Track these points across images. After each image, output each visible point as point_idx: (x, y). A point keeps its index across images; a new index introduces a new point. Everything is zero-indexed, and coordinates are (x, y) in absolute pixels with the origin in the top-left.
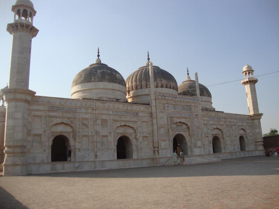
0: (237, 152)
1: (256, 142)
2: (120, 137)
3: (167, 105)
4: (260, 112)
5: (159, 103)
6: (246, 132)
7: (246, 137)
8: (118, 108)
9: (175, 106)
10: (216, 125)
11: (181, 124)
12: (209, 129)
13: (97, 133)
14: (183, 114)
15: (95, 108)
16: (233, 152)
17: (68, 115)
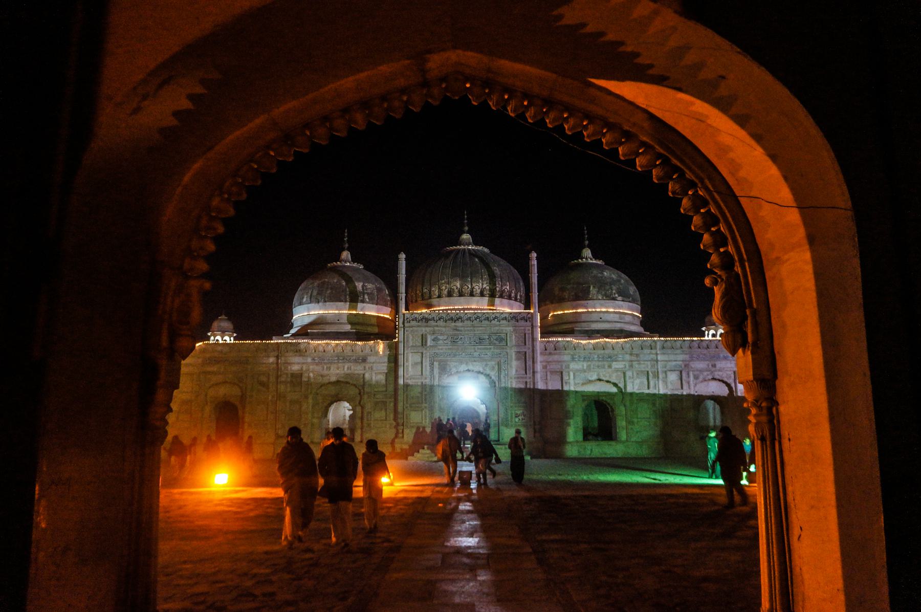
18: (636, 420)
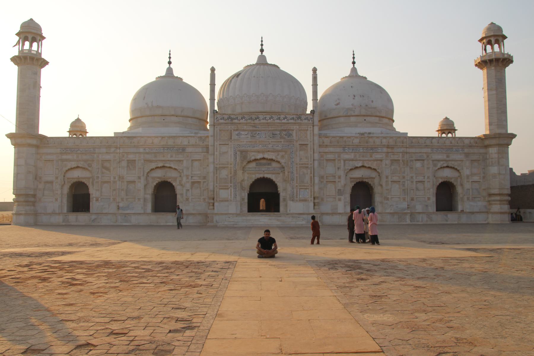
0: (419, 213)
1: (490, 195)
2: (157, 182)
3: (237, 132)
4: (509, 131)
5: (220, 130)
6: (462, 173)
7: (462, 185)
8: (153, 143)
9: (254, 133)
10: (360, 160)
11: (269, 162)
12: (338, 168)
13: (121, 178)
14: (270, 146)
15: (119, 146)
16: (406, 214)
17: (85, 157)
18: (390, 197)
